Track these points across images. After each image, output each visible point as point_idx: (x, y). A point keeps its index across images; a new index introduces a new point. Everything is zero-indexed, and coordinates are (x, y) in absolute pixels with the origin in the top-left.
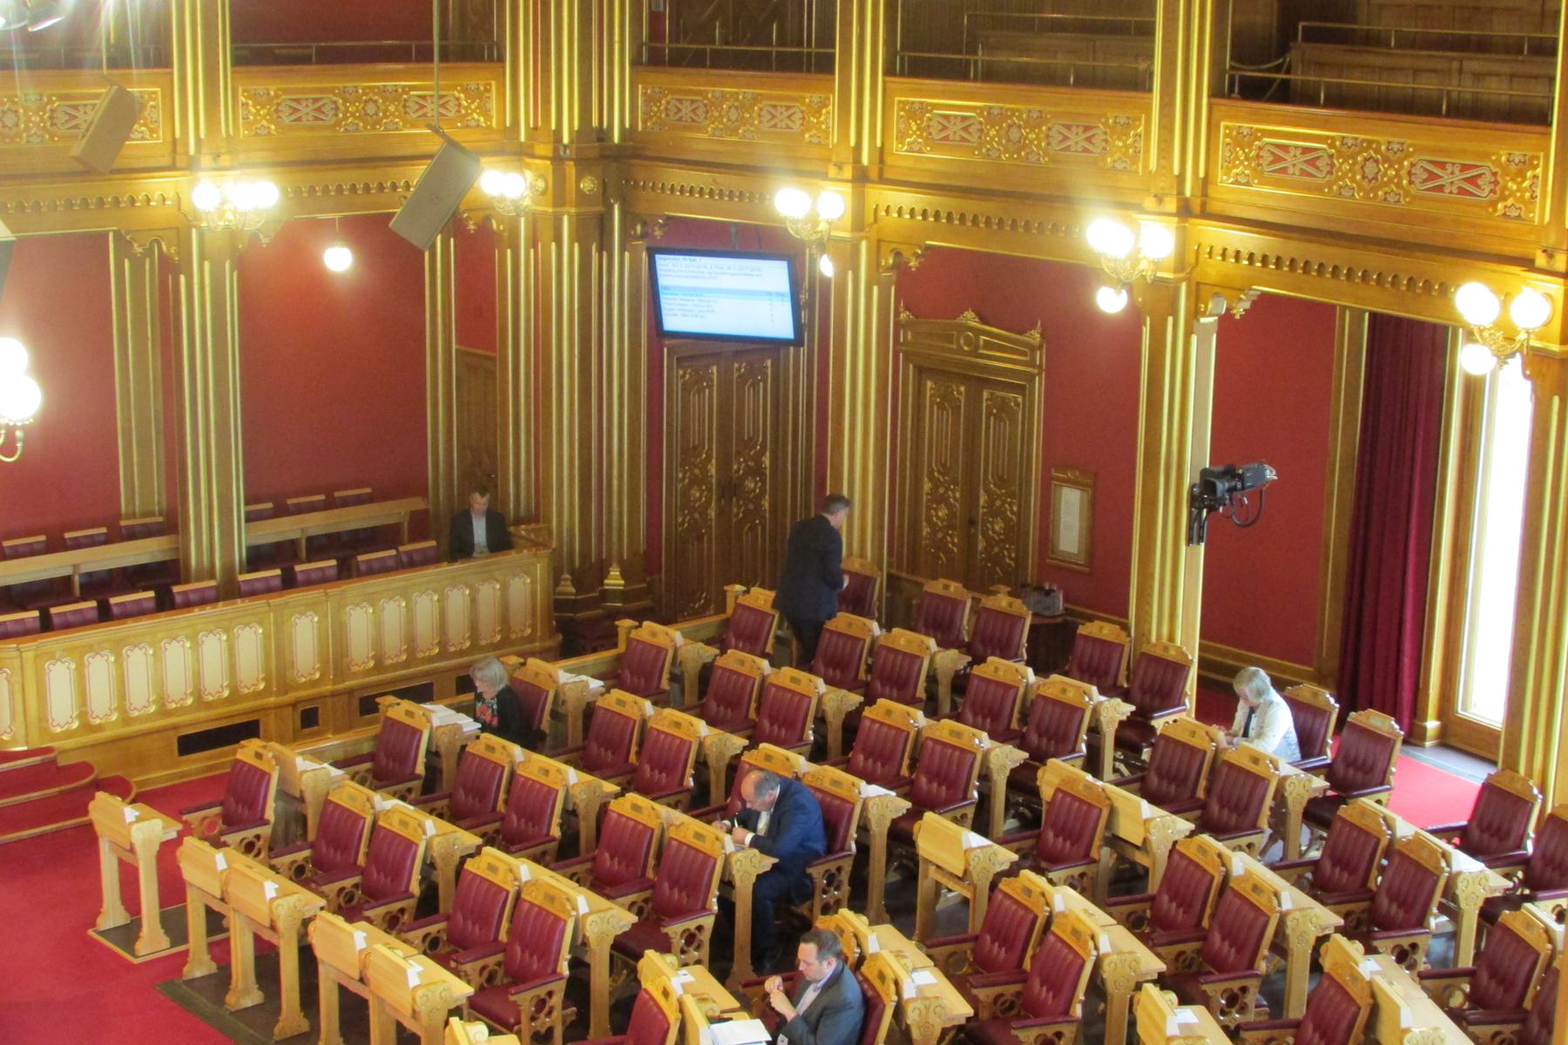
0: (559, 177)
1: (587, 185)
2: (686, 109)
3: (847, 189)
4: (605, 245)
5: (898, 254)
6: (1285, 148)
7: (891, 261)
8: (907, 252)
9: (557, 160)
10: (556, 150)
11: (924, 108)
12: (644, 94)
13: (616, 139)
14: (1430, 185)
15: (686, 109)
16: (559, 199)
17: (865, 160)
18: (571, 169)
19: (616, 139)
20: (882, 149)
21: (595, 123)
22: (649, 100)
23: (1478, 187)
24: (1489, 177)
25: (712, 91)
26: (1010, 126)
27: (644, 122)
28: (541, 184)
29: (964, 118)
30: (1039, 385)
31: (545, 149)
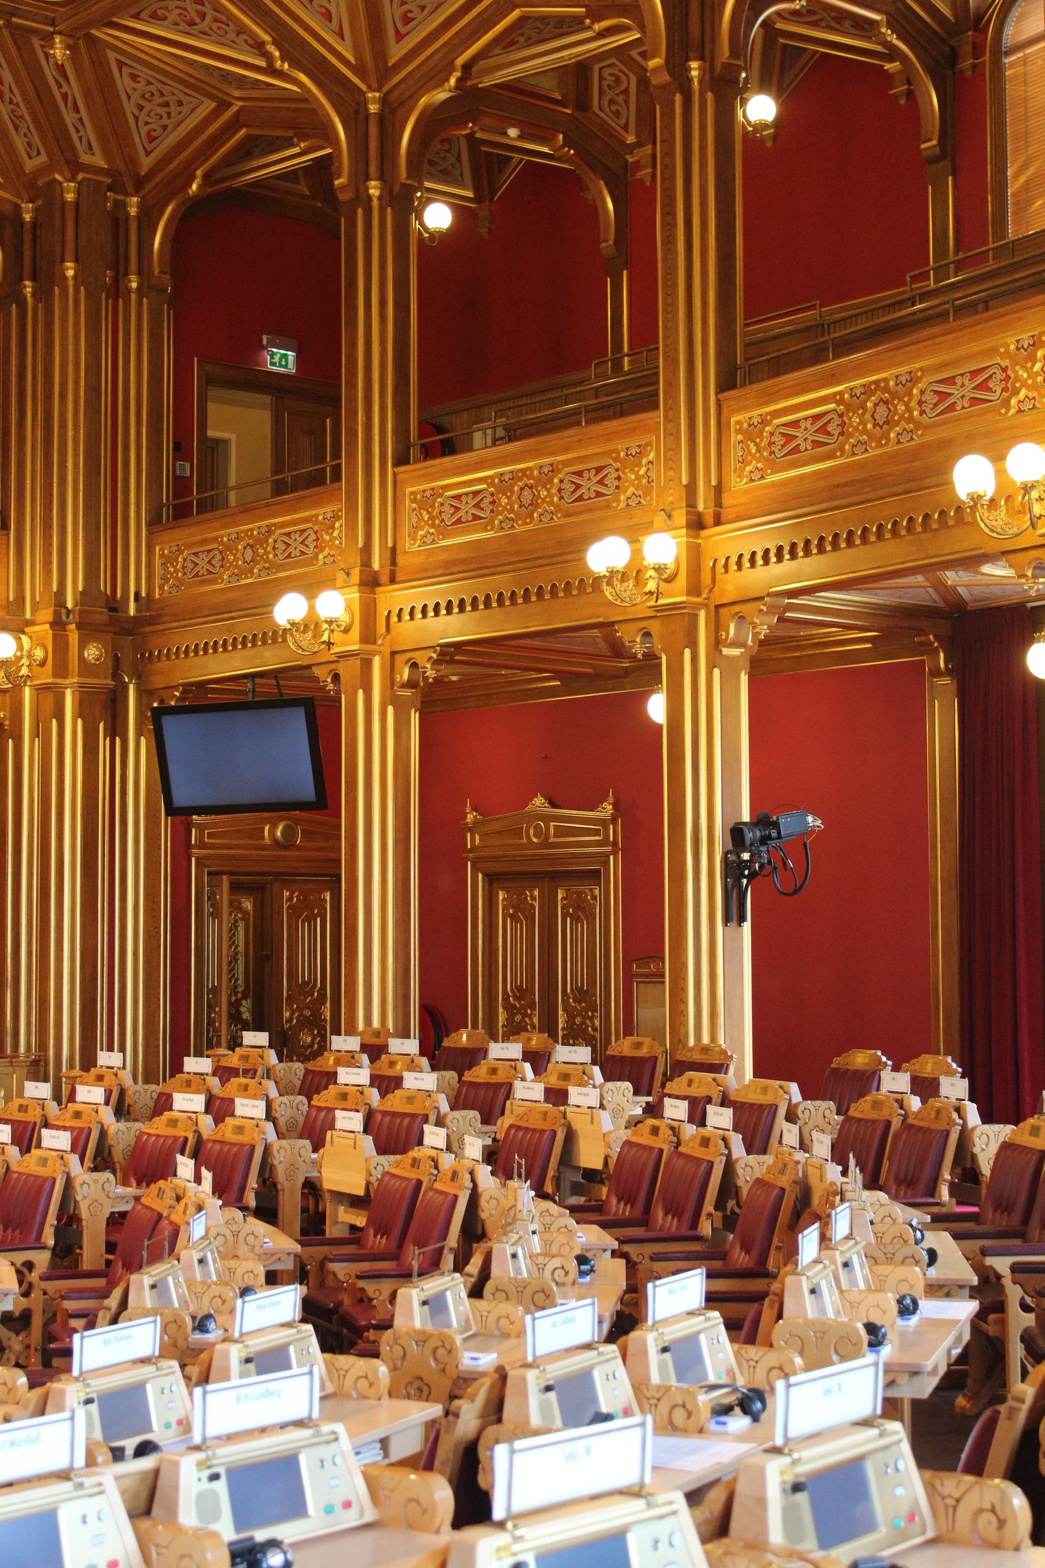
0: (60, 645)
1: (92, 652)
2: (202, 561)
3: (354, 594)
4: (116, 729)
5: (414, 665)
6: (795, 424)
7: (406, 677)
8: (421, 658)
9: (58, 624)
10: (57, 614)
11: (436, 493)
12: (162, 556)
13: (132, 612)
14: (940, 408)
15: (202, 561)
16: (61, 669)
17: (376, 566)
18: (73, 636)
19: (132, 612)
20: (394, 550)
21: (104, 585)
22: (167, 561)
23: (990, 390)
24: (1000, 375)
25: (226, 534)
26: (522, 489)
27: (161, 587)
28: (39, 654)
29: (475, 494)
30: (614, 866)
31: (46, 614)
